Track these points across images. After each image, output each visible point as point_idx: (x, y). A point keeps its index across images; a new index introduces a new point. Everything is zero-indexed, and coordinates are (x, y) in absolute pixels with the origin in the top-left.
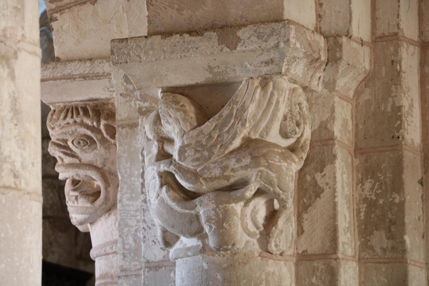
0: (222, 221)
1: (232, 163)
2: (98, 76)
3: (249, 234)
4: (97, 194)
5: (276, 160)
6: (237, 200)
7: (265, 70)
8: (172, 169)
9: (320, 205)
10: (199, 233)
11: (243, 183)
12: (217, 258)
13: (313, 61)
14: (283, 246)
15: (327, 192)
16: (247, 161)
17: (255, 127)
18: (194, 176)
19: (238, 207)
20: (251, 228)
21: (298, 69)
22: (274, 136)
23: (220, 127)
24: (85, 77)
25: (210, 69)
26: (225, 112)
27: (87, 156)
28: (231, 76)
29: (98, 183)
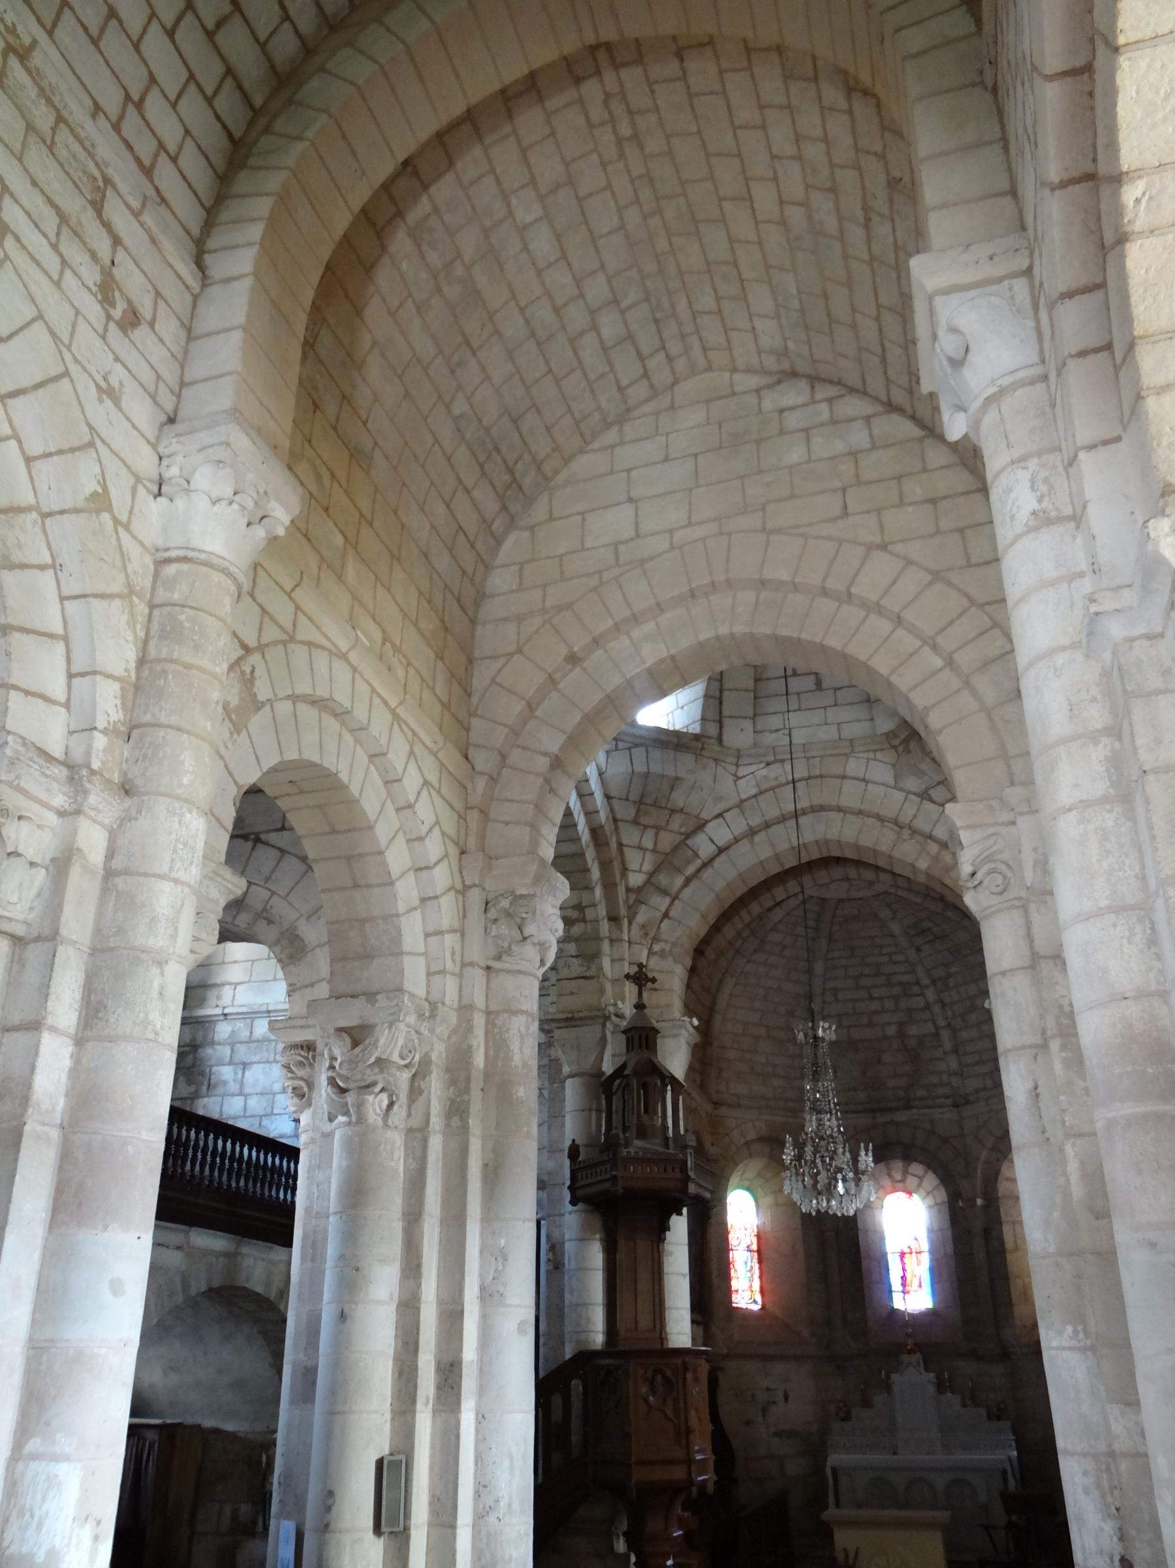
0: (360, 1106)
1: (368, 1071)
2: (309, 1027)
3: (378, 1115)
4: (304, 1096)
5: (393, 1071)
6: (370, 1094)
7: (391, 1018)
8: (334, 1075)
9: (422, 1100)
10: (346, 1113)
11: (374, 1084)
12: (357, 1129)
13: (421, 1016)
14: (397, 1123)
15: (425, 1093)
16: (377, 1070)
17: (384, 1052)
18: (346, 1079)
19: (371, 1098)
20: (378, 1111)
21: (411, 1019)
22: (395, 1057)
23: (363, 1051)
24: (302, 1027)
25: (361, 1017)
26: (367, 1042)
27: (300, 1073)
28: (372, 1021)
29: (306, 1089)
